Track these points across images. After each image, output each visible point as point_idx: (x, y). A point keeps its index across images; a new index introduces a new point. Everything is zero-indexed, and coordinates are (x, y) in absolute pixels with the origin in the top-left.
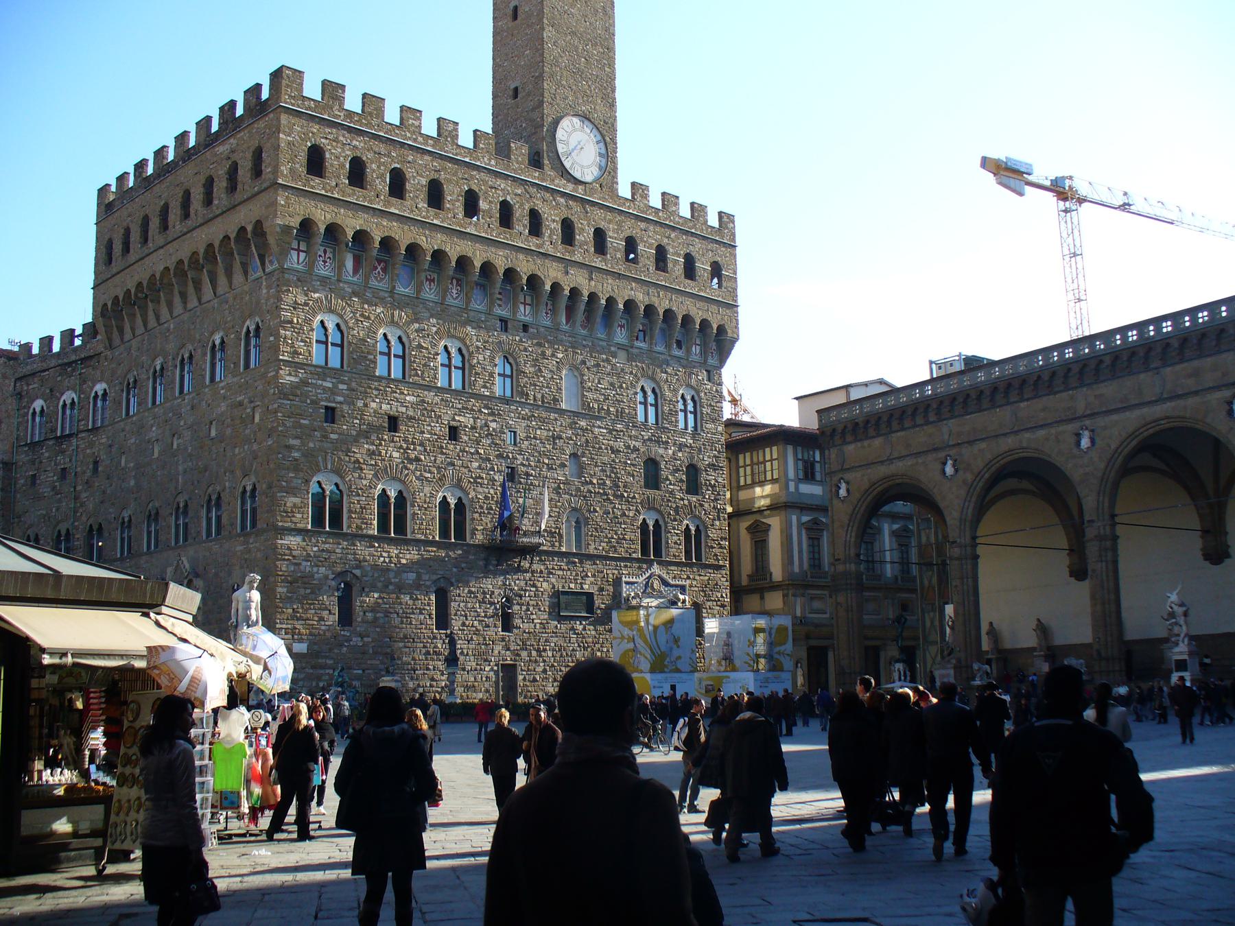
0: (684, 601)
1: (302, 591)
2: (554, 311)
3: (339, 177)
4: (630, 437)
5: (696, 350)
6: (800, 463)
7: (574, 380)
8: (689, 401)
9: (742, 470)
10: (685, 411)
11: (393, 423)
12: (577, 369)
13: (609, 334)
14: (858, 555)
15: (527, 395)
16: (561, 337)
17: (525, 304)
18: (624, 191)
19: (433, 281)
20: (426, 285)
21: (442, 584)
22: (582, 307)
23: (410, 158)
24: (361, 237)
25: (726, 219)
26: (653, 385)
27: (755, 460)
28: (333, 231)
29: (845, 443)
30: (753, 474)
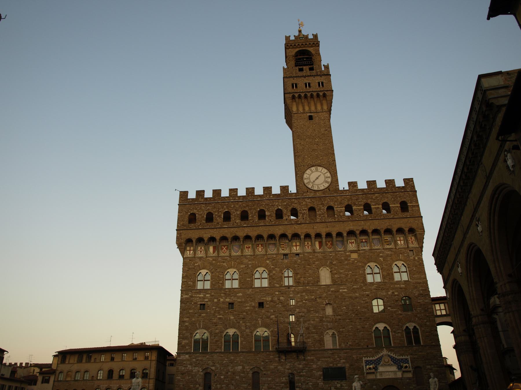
0: (406, 367)
1: (187, 378)
3: (201, 221)
5: (401, 243)
11: (231, 304)
16: (316, 255)
17: (296, 246)
19: (250, 247)
20: (247, 250)
21: (256, 370)
22: (324, 240)
23: (232, 206)
24: (212, 239)
25: (409, 182)
28: (200, 240)
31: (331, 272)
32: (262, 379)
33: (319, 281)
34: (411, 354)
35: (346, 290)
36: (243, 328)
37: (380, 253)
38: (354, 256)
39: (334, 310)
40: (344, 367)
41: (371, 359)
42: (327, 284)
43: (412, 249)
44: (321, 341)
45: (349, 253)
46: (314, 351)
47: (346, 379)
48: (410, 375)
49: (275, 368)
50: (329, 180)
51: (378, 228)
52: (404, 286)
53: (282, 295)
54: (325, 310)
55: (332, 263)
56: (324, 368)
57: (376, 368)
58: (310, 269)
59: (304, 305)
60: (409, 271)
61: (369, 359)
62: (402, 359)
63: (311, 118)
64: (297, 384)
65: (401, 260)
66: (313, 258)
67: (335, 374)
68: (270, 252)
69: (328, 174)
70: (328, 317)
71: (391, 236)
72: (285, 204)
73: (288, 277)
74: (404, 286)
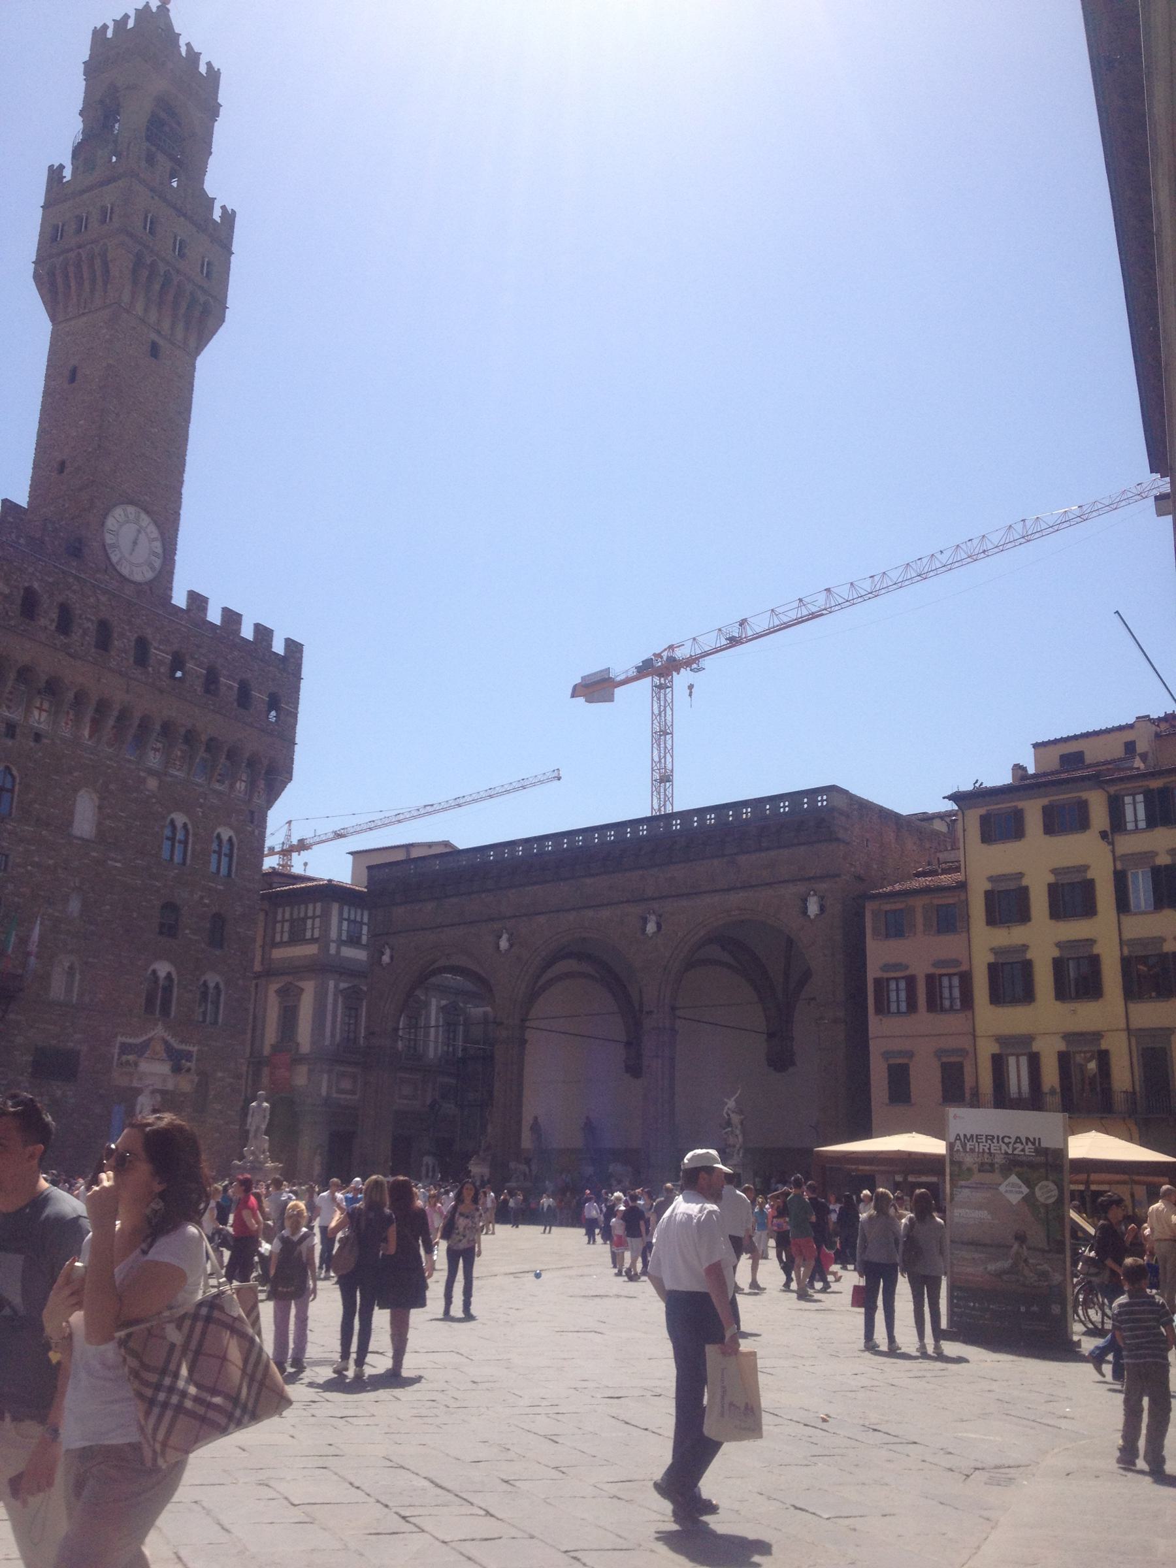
0: (189, 1070)
5: (241, 786)
6: (345, 923)
9: (278, 926)
10: (219, 853)
14: (396, 1029)
17: (40, 709)
18: (179, 599)
22: (111, 722)
25: (295, 648)
27: (295, 916)
30: (291, 932)
31: (100, 808)
35: (118, 865)
38: (152, 783)
50: (157, 563)
52: (221, 887)
57: (136, 1064)
62: (183, 1051)
63: (154, 350)
65: (232, 828)
69: (158, 546)
72: (51, 580)
74: (221, 887)
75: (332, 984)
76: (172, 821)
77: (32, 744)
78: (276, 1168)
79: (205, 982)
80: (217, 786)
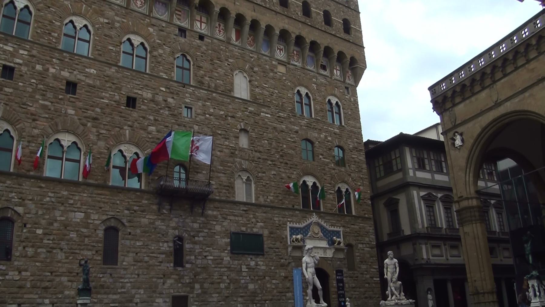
0: (339, 243)
2: (226, 30)
4: (290, 122)
5: (337, 73)
7: (244, 79)
8: (334, 105)
10: (332, 112)
11: (71, 87)
12: (246, 72)
13: (271, 52)
15: (203, 83)
16: (231, 48)
17: (201, 22)
21: (113, 223)
22: (247, 28)
26: (306, 91)
29: (454, 105)
31: (250, 81)
32: (123, 243)
33: (233, 91)
34: (344, 226)
35: (269, 116)
36: (93, 137)
37: (314, 77)
38: (282, 69)
39: (252, 142)
40: (261, 236)
41: (297, 225)
42: (242, 98)
43: (347, 86)
44: (231, 187)
45: (277, 63)
46: (220, 201)
47: (263, 255)
48: (341, 256)
49: (150, 223)
51: (318, 41)
52: (338, 131)
53: (171, 95)
54: (238, 137)
55: (252, 69)
56: (234, 233)
58: (220, 67)
59: (207, 121)
60: (344, 113)
61: (295, 225)
64: (188, 257)
65: (335, 96)
66: (226, 52)
67: (246, 244)
68: (155, 14)
70: (242, 150)
71: (327, 60)
73: (182, 68)
75: (415, 193)
76: (298, 91)
77: (198, 41)
78: (411, 303)
79: (339, 188)
80: (322, 72)
